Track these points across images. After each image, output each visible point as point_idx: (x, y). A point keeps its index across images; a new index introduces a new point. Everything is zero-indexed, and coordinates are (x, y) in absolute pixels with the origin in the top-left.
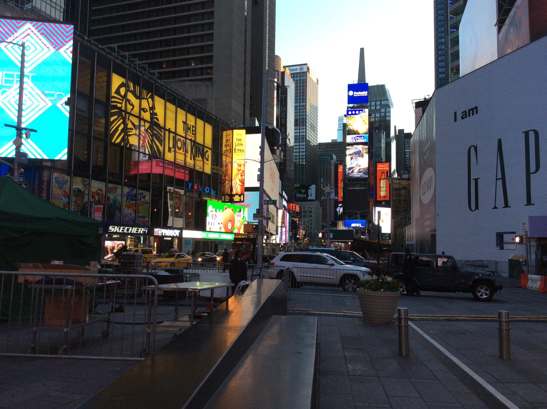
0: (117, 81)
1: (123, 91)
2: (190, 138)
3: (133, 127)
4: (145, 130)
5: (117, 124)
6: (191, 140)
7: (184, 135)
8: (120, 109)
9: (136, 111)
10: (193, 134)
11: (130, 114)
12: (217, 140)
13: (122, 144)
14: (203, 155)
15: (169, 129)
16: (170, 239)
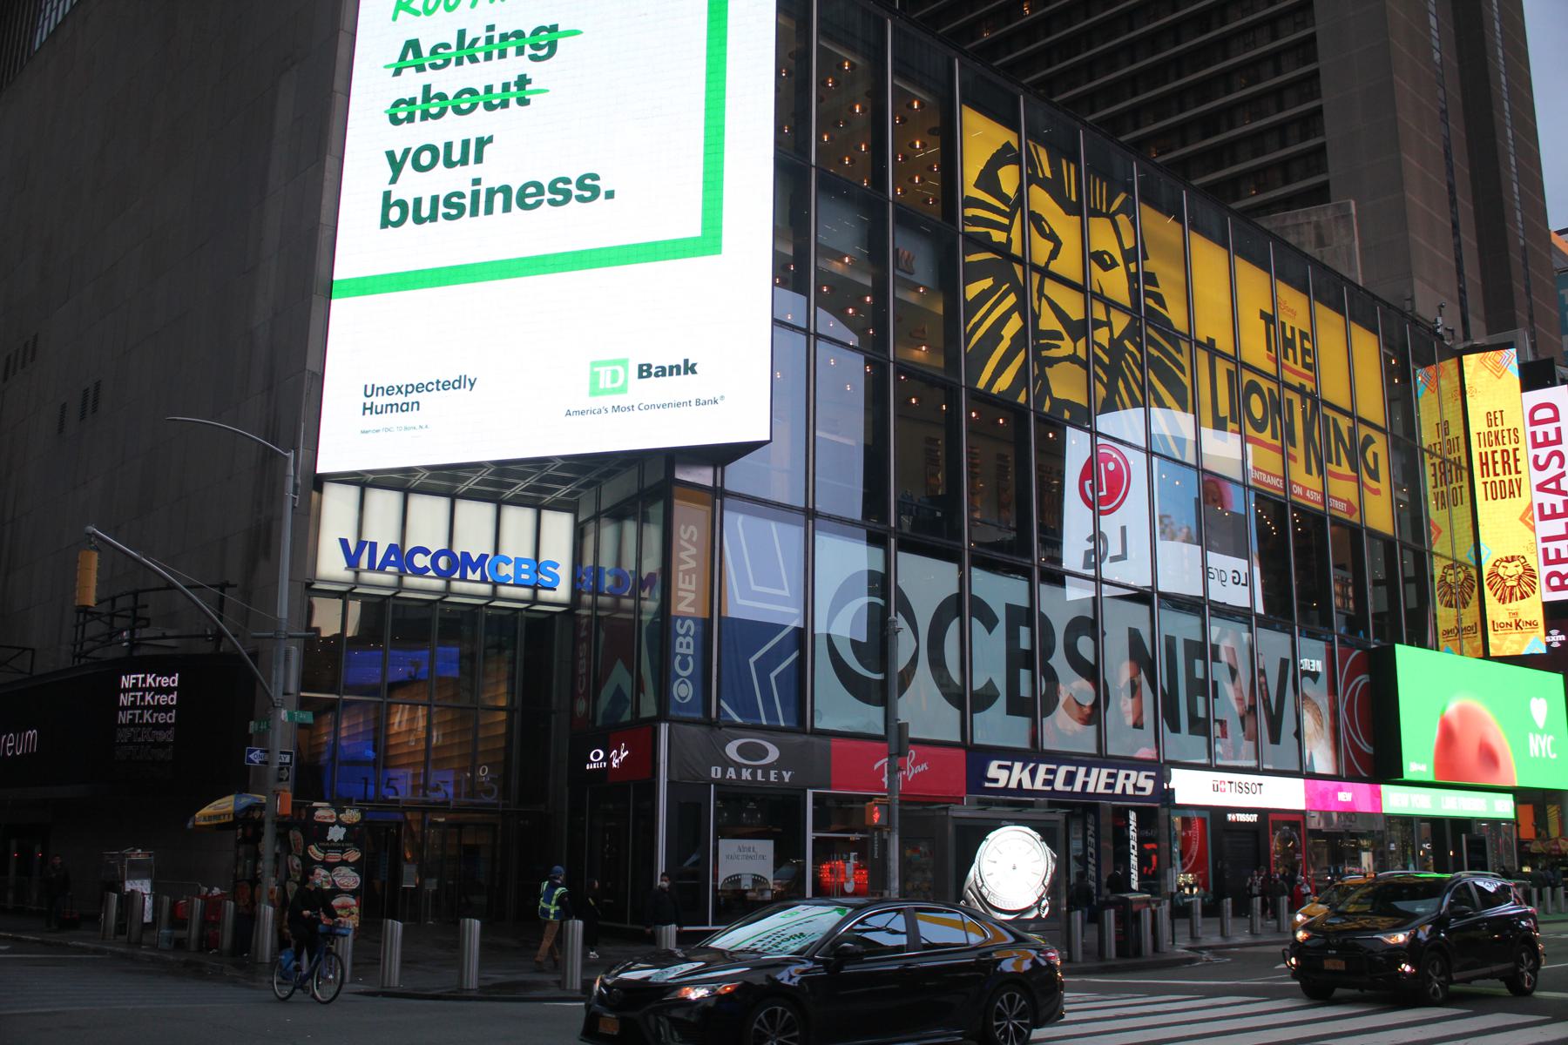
0: (980, 138)
1: (1008, 178)
2: (1295, 380)
3: (1058, 327)
4: (1111, 339)
5: (993, 314)
6: (1300, 390)
7: (1270, 368)
8: (1003, 250)
9: (1069, 264)
10: (1306, 366)
11: (1045, 273)
12: (1400, 397)
13: (1022, 399)
14: (1356, 454)
15: (1211, 341)
16: (1253, 818)
